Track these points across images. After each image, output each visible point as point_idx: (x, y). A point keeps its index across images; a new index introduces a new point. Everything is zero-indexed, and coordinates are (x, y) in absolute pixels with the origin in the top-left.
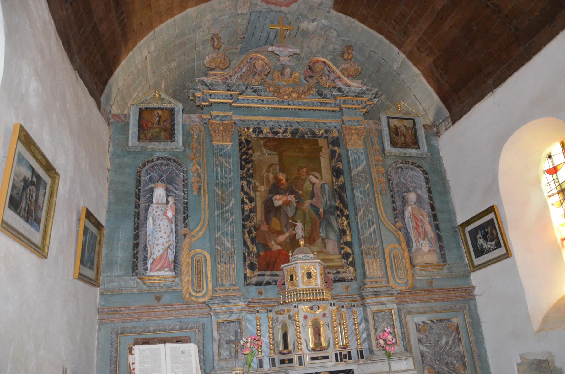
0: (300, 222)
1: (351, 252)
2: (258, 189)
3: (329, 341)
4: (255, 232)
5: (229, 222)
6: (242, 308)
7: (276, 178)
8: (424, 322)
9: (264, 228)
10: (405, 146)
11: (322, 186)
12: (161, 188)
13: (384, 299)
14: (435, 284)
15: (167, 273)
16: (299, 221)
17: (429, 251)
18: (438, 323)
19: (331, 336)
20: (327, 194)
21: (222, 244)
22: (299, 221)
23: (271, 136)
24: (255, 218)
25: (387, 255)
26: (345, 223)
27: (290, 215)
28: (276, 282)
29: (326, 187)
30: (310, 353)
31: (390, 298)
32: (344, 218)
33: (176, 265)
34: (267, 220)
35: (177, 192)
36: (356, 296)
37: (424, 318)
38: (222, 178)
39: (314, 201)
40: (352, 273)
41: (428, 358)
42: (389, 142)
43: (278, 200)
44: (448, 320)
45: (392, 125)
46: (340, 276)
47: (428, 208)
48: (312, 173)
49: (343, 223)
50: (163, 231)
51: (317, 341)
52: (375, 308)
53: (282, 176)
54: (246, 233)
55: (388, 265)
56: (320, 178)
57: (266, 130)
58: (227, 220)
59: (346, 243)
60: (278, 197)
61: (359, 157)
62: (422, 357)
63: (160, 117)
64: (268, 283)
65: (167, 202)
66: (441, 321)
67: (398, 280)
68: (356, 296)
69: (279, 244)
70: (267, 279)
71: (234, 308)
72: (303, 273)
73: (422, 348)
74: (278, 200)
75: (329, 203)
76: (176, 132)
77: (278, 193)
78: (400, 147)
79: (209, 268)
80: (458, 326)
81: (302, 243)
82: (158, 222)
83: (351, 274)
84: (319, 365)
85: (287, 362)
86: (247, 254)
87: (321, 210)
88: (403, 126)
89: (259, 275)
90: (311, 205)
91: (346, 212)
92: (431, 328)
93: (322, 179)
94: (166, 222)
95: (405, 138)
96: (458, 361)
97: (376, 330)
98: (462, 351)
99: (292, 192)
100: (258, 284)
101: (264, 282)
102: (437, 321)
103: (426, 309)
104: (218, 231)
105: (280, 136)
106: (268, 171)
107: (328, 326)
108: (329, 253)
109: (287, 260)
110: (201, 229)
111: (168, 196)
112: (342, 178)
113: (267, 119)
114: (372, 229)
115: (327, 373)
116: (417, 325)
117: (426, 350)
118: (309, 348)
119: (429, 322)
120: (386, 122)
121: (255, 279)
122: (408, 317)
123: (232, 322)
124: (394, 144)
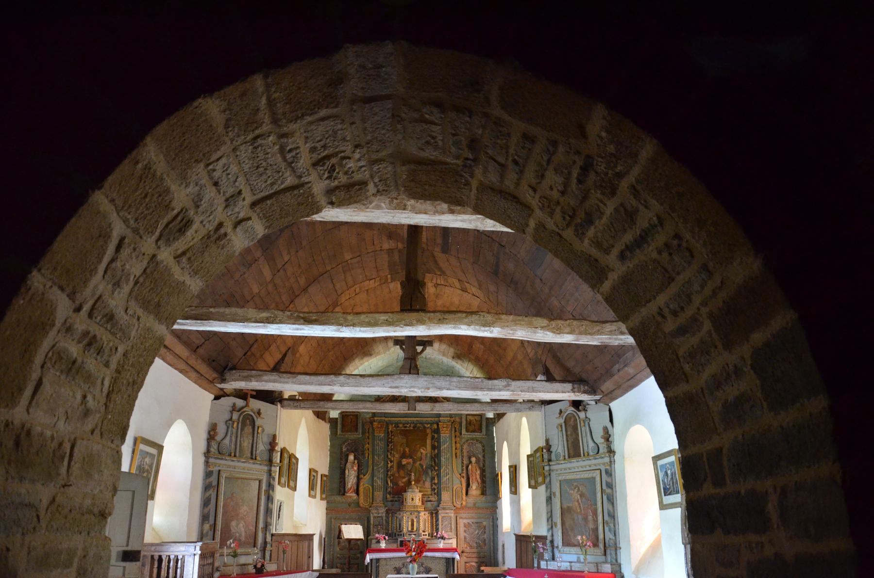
7: (404, 450)
8: (468, 523)
9: (397, 475)
11: (426, 454)
13: (448, 511)
14: (477, 505)
15: (354, 495)
23: (403, 428)
25: (454, 490)
28: (399, 500)
29: (428, 455)
34: (398, 472)
37: (469, 521)
39: (421, 462)
43: (404, 462)
45: (468, 420)
46: (429, 499)
47: (481, 465)
52: (443, 515)
53: (407, 450)
55: (454, 495)
57: (401, 426)
59: (435, 484)
60: (404, 460)
63: (351, 419)
64: (396, 501)
66: (477, 523)
71: (380, 511)
74: (404, 462)
77: (405, 458)
78: (471, 432)
81: (413, 483)
87: (424, 467)
90: (420, 464)
91: (436, 468)
92: (471, 526)
94: (353, 472)
99: (411, 458)
105: (408, 428)
106: (401, 447)
108: (425, 488)
109: (405, 491)
111: (355, 459)
112: (436, 451)
116: (464, 523)
121: (390, 499)
122: (461, 520)
124: (467, 431)
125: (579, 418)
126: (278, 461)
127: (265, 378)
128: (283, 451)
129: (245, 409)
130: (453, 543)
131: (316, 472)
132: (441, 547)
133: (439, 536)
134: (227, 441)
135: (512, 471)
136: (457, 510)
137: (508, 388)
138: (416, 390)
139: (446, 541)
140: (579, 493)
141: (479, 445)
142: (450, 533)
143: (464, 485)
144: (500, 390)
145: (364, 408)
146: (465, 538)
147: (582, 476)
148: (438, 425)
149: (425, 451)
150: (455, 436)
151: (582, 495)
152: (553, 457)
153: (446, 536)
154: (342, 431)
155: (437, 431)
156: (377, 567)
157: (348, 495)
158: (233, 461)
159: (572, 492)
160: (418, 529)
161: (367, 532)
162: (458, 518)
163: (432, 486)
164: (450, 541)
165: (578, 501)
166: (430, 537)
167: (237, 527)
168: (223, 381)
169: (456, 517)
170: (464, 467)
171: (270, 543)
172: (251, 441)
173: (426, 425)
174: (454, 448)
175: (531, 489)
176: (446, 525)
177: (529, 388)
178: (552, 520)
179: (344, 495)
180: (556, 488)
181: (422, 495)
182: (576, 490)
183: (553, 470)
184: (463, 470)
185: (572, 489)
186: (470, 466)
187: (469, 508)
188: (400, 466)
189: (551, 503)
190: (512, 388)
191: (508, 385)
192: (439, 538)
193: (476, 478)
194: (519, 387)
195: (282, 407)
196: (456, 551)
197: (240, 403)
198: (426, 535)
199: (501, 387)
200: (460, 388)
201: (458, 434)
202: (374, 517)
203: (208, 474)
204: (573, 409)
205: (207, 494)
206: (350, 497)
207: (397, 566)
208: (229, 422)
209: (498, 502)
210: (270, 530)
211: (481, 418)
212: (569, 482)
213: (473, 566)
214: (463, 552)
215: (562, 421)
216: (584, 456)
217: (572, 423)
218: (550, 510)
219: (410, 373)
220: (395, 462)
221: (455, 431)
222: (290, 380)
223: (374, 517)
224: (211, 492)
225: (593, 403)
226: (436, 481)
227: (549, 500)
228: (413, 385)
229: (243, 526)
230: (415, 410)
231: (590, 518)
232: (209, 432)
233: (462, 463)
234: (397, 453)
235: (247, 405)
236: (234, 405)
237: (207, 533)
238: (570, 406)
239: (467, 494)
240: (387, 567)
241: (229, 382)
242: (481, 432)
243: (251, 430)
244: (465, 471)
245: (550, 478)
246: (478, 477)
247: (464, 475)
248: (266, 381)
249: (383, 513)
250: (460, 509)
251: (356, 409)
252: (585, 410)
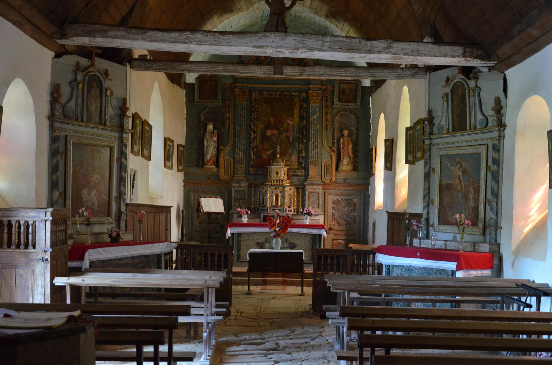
0: (279, 145)
2: (259, 126)
5: (243, 144)
8: (337, 200)
9: (260, 147)
10: (348, 101)
11: (293, 125)
12: (210, 125)
13: (315, 187)
14: (348, 181)
15: (213, 167)
17: (347, 164)
18: (345, 201)
20: (295, 130)
21: (238, 154)
23: (268, 96)
27: (274, 141)
28: (263, 174)
29: (296, 126)
31: (319, 187)
33: (217, 164)
35: (219, 126)
38: (240, 121)
41: (336, 217)
42: (337, 99)
43: (269, 133)
44: (351, 200)
45: (342, 88)
46: (296, 173)
47: (354, 139)
48: (289, 118)
49: (301, 146)
50: (211, 147)
52: (310, 191)
53: (272, 120)
55: (323, 170)
56: (293, 121)
58: (242, 143)
59: (302, 157)
60: (269, 131)
61: (316, 109)
62: (333, 215)
64: (259, 175)
65: (214, 132)
66: (347, 200)
67: (326, 178)
69: (267, 156)
70: (259, 172)
71: (242, 185)
73: (333, 211)
74: (269, 133)
75: (295, 135)
76: (218, 94)
77: (270, 129)
78: (344, 102)
79: (232, 166)
80: (356, 203)
82: (209, 142)
87: (291, 139)
88: (348, 88)
90: (286, 136)
91: (304, 141)
92: (341, 202)
93: (294, 122)
94: (213, 143)
95: (348, 96)
96: (351, 220)
97: (309, 201)
98: (355, 215)
99: (277, 128)
100: (254, 174)
102: (345, 199)
103: (339, 193)
104: (237, 148)
108: (292, 162)
109: (270, 165)
110: (229, 147)
111: (214, 130)
112: (305, 122)
113: (267, 86)
114: (316, 151)
117: (335, 212)
119: (340, 200)
120: (338, 85)
121: (253, 173)
122: (329, 196)
123: (241, 191)
124: (340, 100)
125: (468, 87)
126: (130, 128)
127: (112, 33)
128: (135, 116)
129: (90, 69)
130: (320, 220)
131: (172, 141)
132: (308, 223)
133: (305, 212)
134: (72, 104)
135: (389, 146)
136: (325, 185)
137: (389, 50)
138: (283, 50)
139: (313, 218)
140: (462, 169)
141: (353, 117)
142: (317, 210)
143: (334, 159)
144: (380, 53)
145: (225, 71)
146: (333, 215)
147: (466, 152)
148: (307, 94)
149: (293, 122)
150: (327, 107)
151: (464, 172)
152: (435, 130)
153: (312, 212)
154: (200, 98)
155: (306, 100)
156: (239, 242)
157: (207, 167)
158: (80, 126)
159: (454, 168)
160: (283, 204)
161: (228, 206)
162: (326, 194)
163: (299, 160)
164: (317, 218)
165: (459, 178)
166: (295, 213)
167: (89, 195)
168: (64, 36)
169: (325, 193)
170: (335, 141)
171: (124, 213)
172: (99, 105)
173: (294, 94)
174: (324, 120)
175: (408, 165)
176: (313, 201)
177: (413, 51)
178: (429, 197)
179: (203, 166)
180: (436, 163)
181: (288, 169)
182: (458, 166)
183: (434, 145)
184: (333, 143)
185: (453, 165)
186: (342, 140)
187: (340, 184)
188: (264, 138)
189: (429, 180)
190: (393, 51)
191: (390, 47)
192: (305, 214)
193: (348, 153)
194: (402, 50)
195: (132, 67)
196: (324, 228)
197: (84, 62)
198: (291, 211)
199: (381, 49)
200: (334, 50)
201: (329, 103)
202: (236, 191)
203: (54, 140)
204: (462, 77)
205: (55, 161)
206: (210, 169)
207: (260, 241)
208: (73, 83)
209: (371, 179)
210: (124, 200)
211: (357, 87)
212: (451, 157)
213: (341, 243)
214: (330, 229)
215: (448, 90)
216: (470, 129)
217: (459, 92)
218: (427, 187)
219: (277, 31)
220: (258, 132)
221: (327, 101)
222: (140, 36)
223: (236, 191)
224: (58, 158)
225: (486, 70)
226: (304, 155)
227: (427, 176)
228: (280, 44)
229: (96, 195)
230: (282, 75)
231: (471, 196)
232: (52, 94)
233: (333, 136)
234: (261, 124)
235: (92, 65)
236: (78, 63)
237: (58, 200)
238: (459, 73)
239: (337, 169)
240: (250, 242)
241: (69, 38)
242: (356, 102)
243: (98, 93)
244: (335, 145)
245: (430, 152)
246: (350, 151)
247: (335, 149)
248: (113, 37)
249: (245, 187)
250: (329, 184)
251: (215, 71)
252: (476, 78)
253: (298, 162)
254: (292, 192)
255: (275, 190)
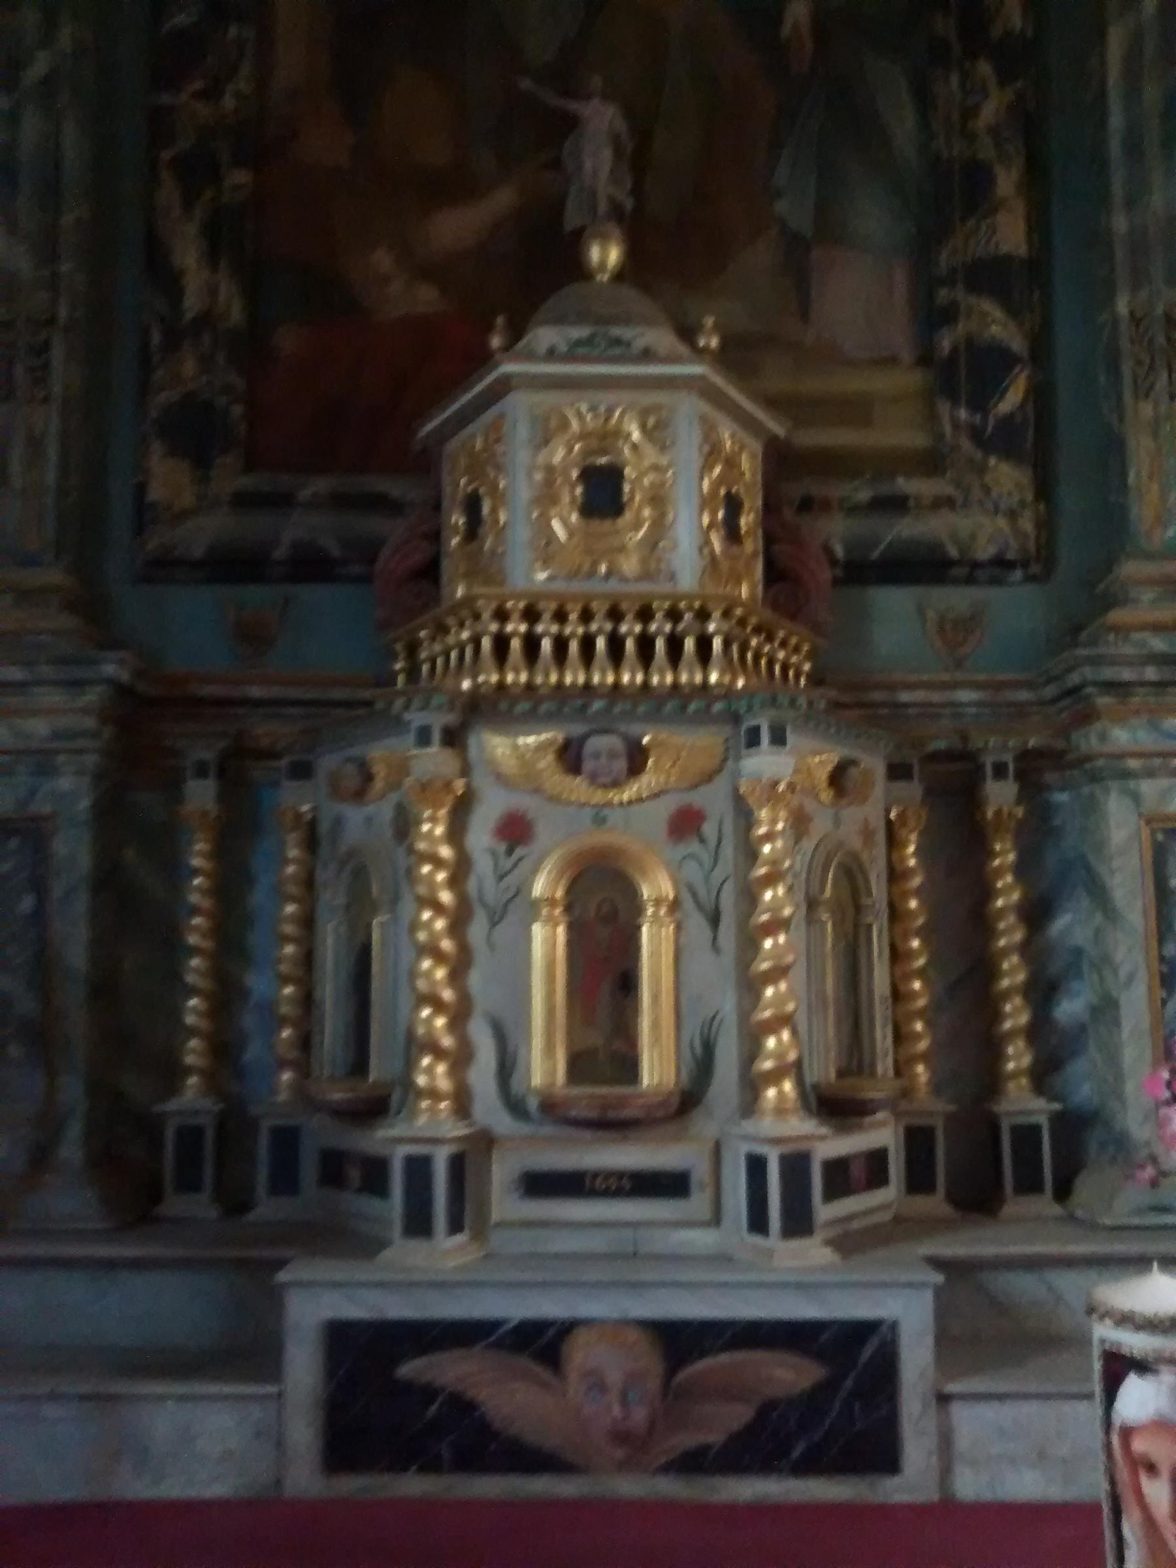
0: (605, 97)
1: (1017, 344)
3: (708, 1048)
4: (240, 177)
6: (57, 735)
16: (597, 81)
19: (728, 1004)
22: (597, 81)
24: (246, 69)
26: (990, 111)
28: (369, 550)
30: (524, 1129)
32: (985, 68)
36: (1024, 695)
40: (1012, 515)
49: (970, 113)
51: (595, 1039)
54: (165, 176)
68: (1024, 695)
72: (550, 470)
83: (1002, 522)
84: (596, 1242)
85: (355, 1175)
86: (156, 338)
89: (243, 501)
101: (280, 553)
107: (714, 920)
115: (633, 1335)
118: (516, 1085)
166: (935, 1204)
253: (925, 359)
254: (867, 835)
255: (577, 787)
